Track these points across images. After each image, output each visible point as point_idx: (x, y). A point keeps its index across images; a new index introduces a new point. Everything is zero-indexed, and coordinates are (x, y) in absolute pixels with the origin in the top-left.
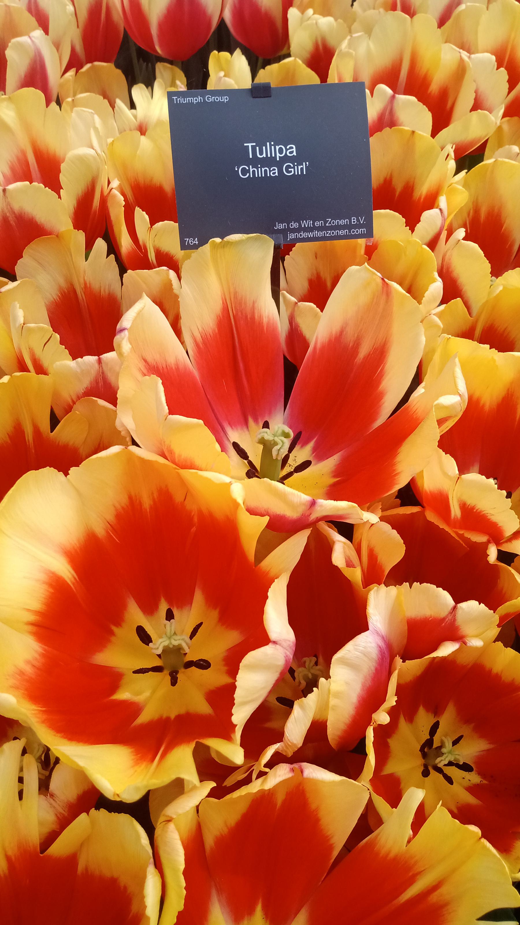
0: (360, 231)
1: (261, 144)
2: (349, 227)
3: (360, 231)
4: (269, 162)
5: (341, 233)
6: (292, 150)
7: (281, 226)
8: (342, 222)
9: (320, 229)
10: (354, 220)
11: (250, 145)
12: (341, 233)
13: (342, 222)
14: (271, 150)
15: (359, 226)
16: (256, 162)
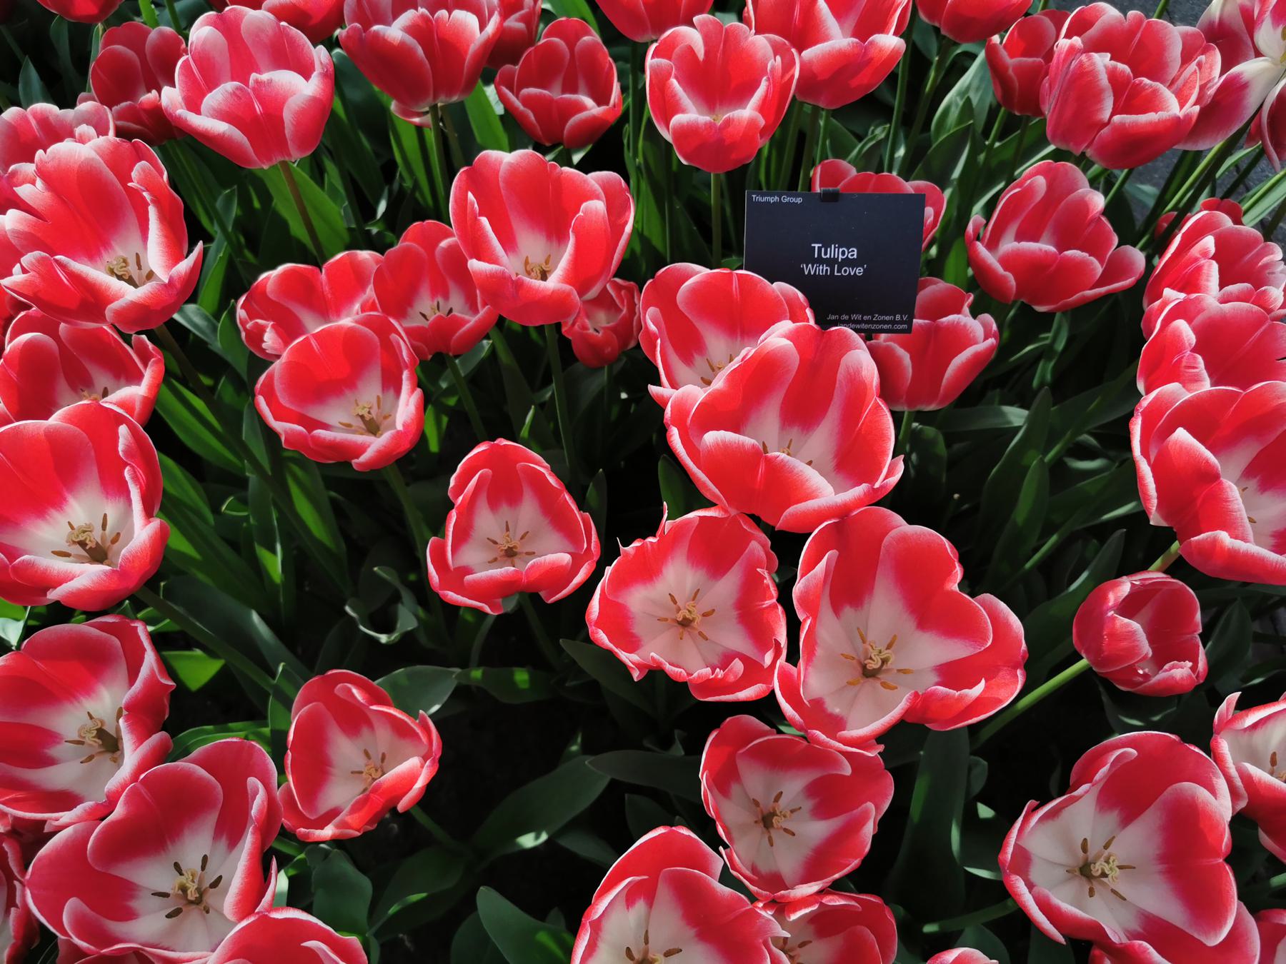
0: (902, 327)
1: (826, 246)
2: (893, 322)
3: (902, 327)
4: (831, 262)
5: (885, 327)
6: (853, 253)
7: (833, 317)
8: (887, 318)
9: (867, 322)
10: (898, 317)
11: (817, 246)
12: (885, 327)
13: (887, 318)
14: (835, 252)
15: (902, 322)
16: (820, 261)
